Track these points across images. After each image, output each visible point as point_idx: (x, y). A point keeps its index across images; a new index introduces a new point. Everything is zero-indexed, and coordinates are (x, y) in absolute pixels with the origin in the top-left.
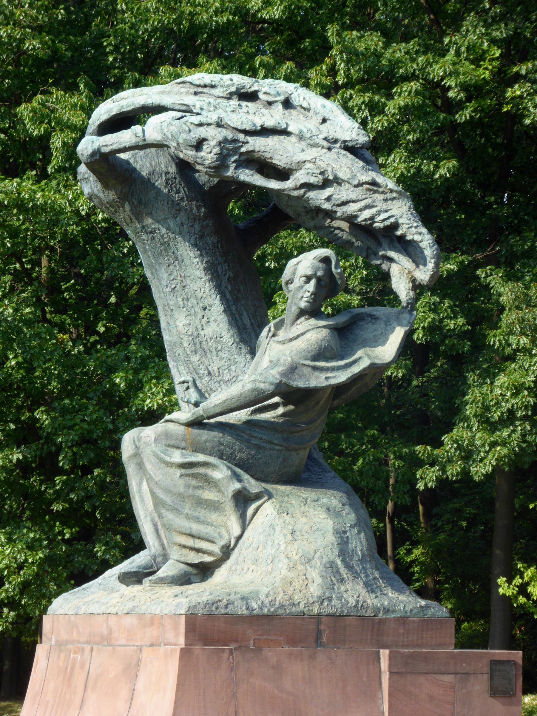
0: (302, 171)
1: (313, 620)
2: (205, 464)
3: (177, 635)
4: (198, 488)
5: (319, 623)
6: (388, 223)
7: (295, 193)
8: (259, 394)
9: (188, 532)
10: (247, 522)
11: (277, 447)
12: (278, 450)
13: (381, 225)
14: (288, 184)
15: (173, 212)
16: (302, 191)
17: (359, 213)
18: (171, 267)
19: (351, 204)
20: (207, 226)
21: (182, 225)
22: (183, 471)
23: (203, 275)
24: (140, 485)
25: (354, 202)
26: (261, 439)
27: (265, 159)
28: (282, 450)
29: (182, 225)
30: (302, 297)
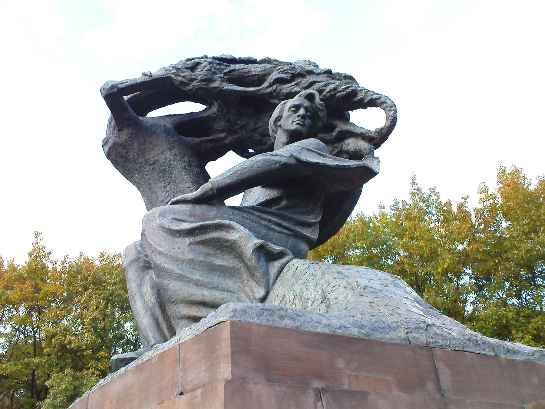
0: (274, 73)
1: (425, 352)
2: (219, 227)
3: (213, 366)
4: (210, 255)
5: (432, 357)
6: (349, 90)
7: (269, 90)
8: (271, 165)
9: (200, 299)
10: (271, 282)
11: (286, 231)
12: (286, 233)
13: (344, 93)
14: (263, 86)
15: (169, 147)
16: (274, 87)
17: (324, 88)
18: (167, 188)
19: (317, 84)
20: (193, 161)
21: (176, 155)
22: (192, 239)
23: (191, 186)
24: (140, 286)
25: (318, 82)
26: (270, 221)
27: (243, 75)
28: (290, 235)
29: (176, 155)
30: (293, 122)
